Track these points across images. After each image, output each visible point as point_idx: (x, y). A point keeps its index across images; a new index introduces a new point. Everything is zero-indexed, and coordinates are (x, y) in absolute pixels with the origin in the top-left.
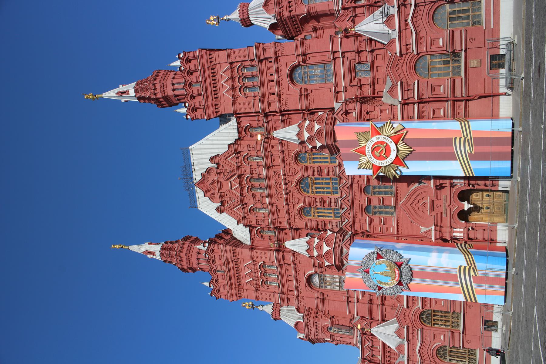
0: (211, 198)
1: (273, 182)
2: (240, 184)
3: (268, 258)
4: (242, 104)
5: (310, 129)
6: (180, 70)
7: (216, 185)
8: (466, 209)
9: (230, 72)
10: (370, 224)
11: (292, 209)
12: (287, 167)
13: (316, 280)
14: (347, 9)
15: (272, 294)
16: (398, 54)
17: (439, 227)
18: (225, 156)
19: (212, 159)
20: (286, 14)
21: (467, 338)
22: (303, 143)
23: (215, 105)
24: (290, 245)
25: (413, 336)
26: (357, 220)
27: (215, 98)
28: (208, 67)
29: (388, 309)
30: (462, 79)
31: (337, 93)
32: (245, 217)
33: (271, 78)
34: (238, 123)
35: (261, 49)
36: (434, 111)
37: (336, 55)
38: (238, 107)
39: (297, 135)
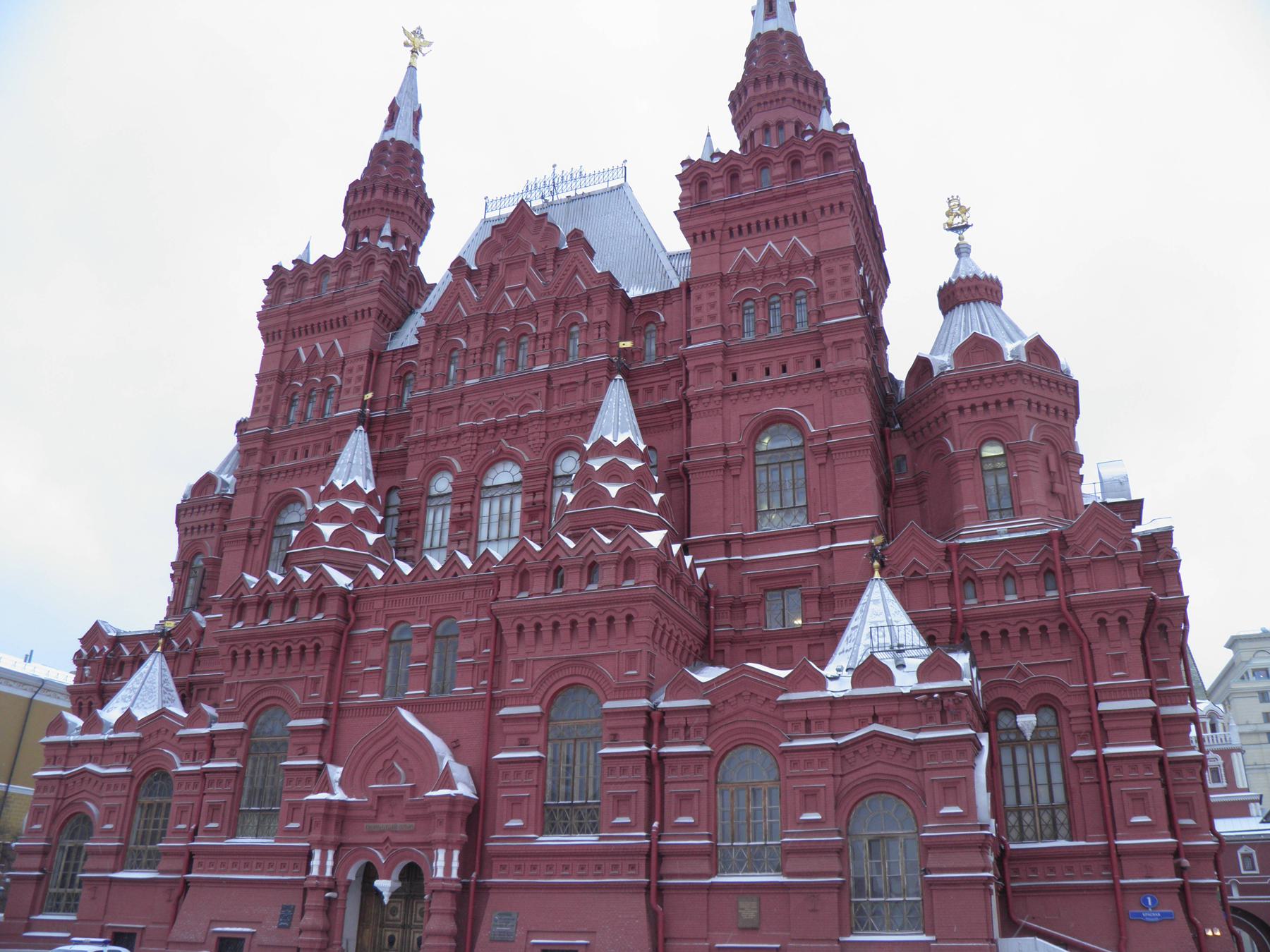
5: (614, 472)
8: (378, 883)
9: (797, 260)
14: (948, 560)
16: (782, 698)
17: (338, 815)
20: (953, 398)
23: (712, 232)
27: (731, 230)
28: (808, 203)
30: (710, 877)
31: (727, 542)
33: (775, 368)
34: (666, 292)
35: (849, 336)
36: (627, 797)
37: (826, 535)
38: (704, 291)
39: (602, 440)
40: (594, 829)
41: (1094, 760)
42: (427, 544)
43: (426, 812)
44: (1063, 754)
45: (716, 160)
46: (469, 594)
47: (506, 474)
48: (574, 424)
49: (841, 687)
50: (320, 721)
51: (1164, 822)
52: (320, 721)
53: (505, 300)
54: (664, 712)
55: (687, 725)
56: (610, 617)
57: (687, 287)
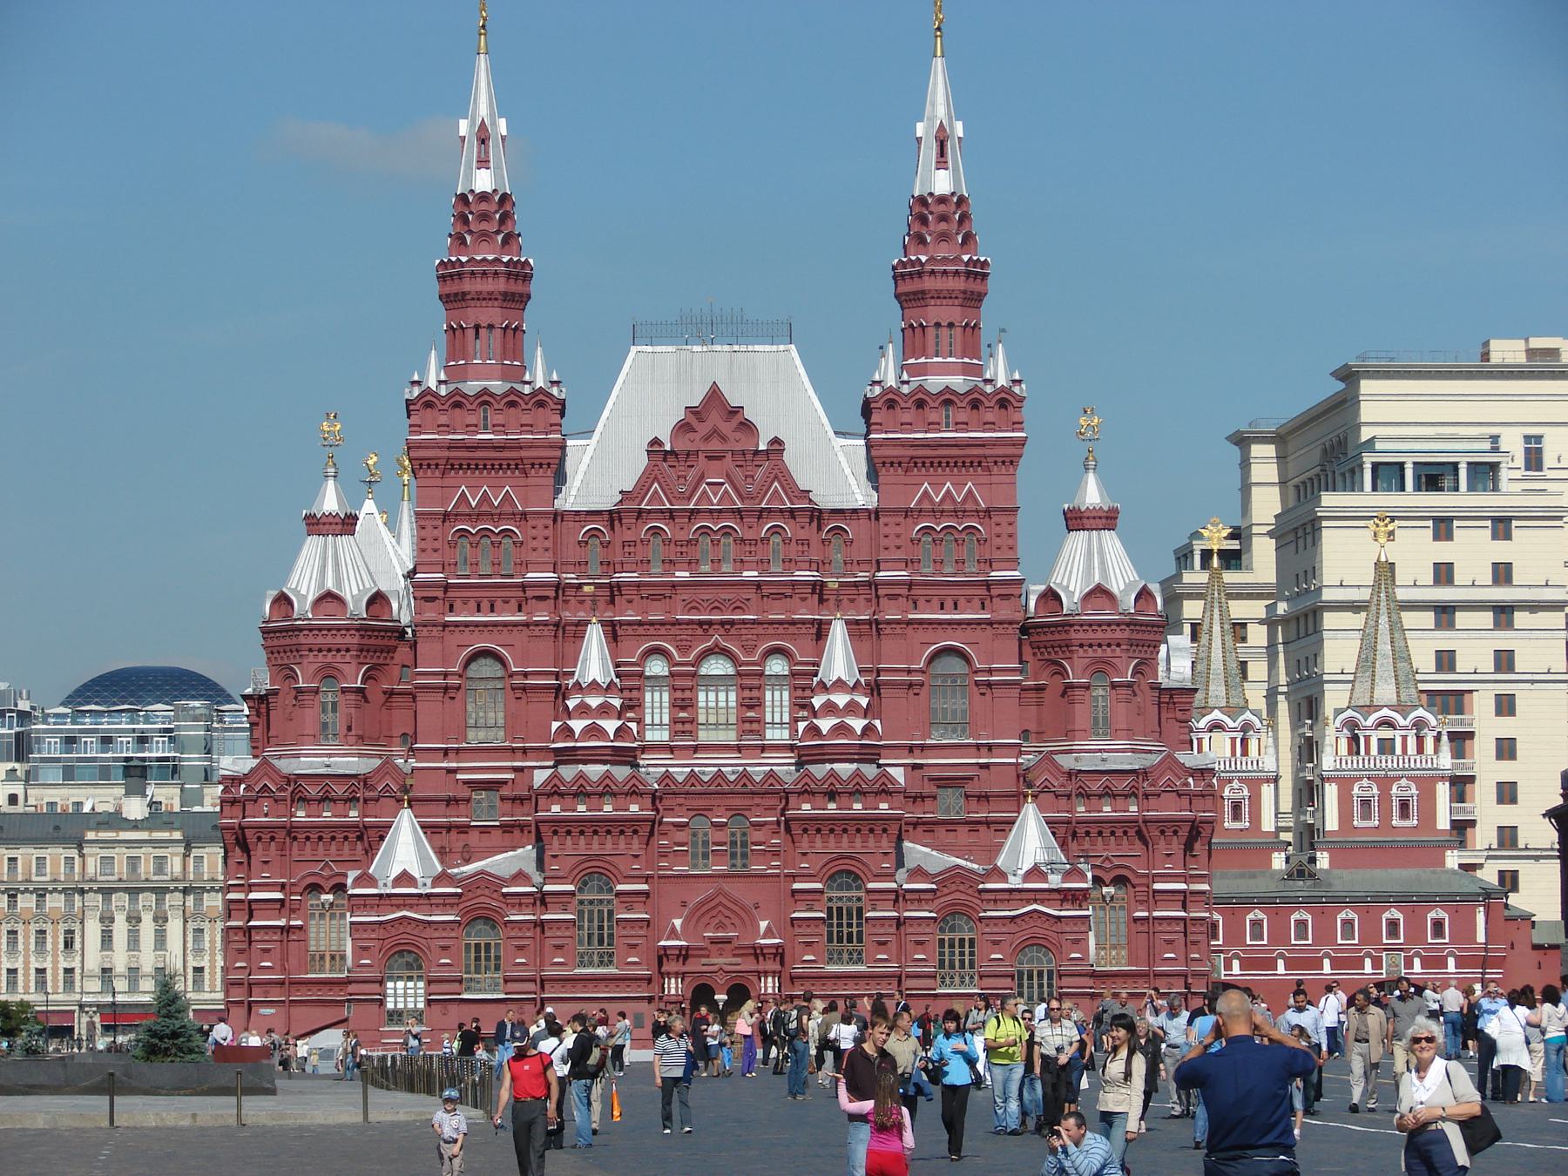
0: (683, 428)
1: (726, 595)
2: (720, 511)
3: (533, 557)
4: (898, 530)
5: (852, 708)
6: (987, 381)
7: (715, 445)
10: (673, 824)
11: (663, 631)
12: (760, 629)
13: (486, 668)
15: (436, 557)
17: (684, 954)
18: (784, 476)
19: (776, 441)
20: (1076, 636)
21: (453, 1008)
22: (823, 687)
24: (595, 636)
25: (437, 905)
26: (681, 801)
29: (443, 838)
31: (911, 749)
32: (640, 511)
33: (949, 603)
34: (855, 511)
36: (884, 943)
37: (984, 751)
39: (839, 680)
40: (859, 961)
41: (1146, 919)
42: (648, 720)
43: (758, 953)
44: (1129, 912)
45: (905, 389)
46: (757, 800)
47: (717, 667)
48: (781, 631)
49: (1015, 882)
50: (645, 887)
51: (1182, 958)
52: (645, 887)
53: (704, 492)
54: (908, 891)
55: (919, 897)
56: (870, 825)
57: (875, 514)
